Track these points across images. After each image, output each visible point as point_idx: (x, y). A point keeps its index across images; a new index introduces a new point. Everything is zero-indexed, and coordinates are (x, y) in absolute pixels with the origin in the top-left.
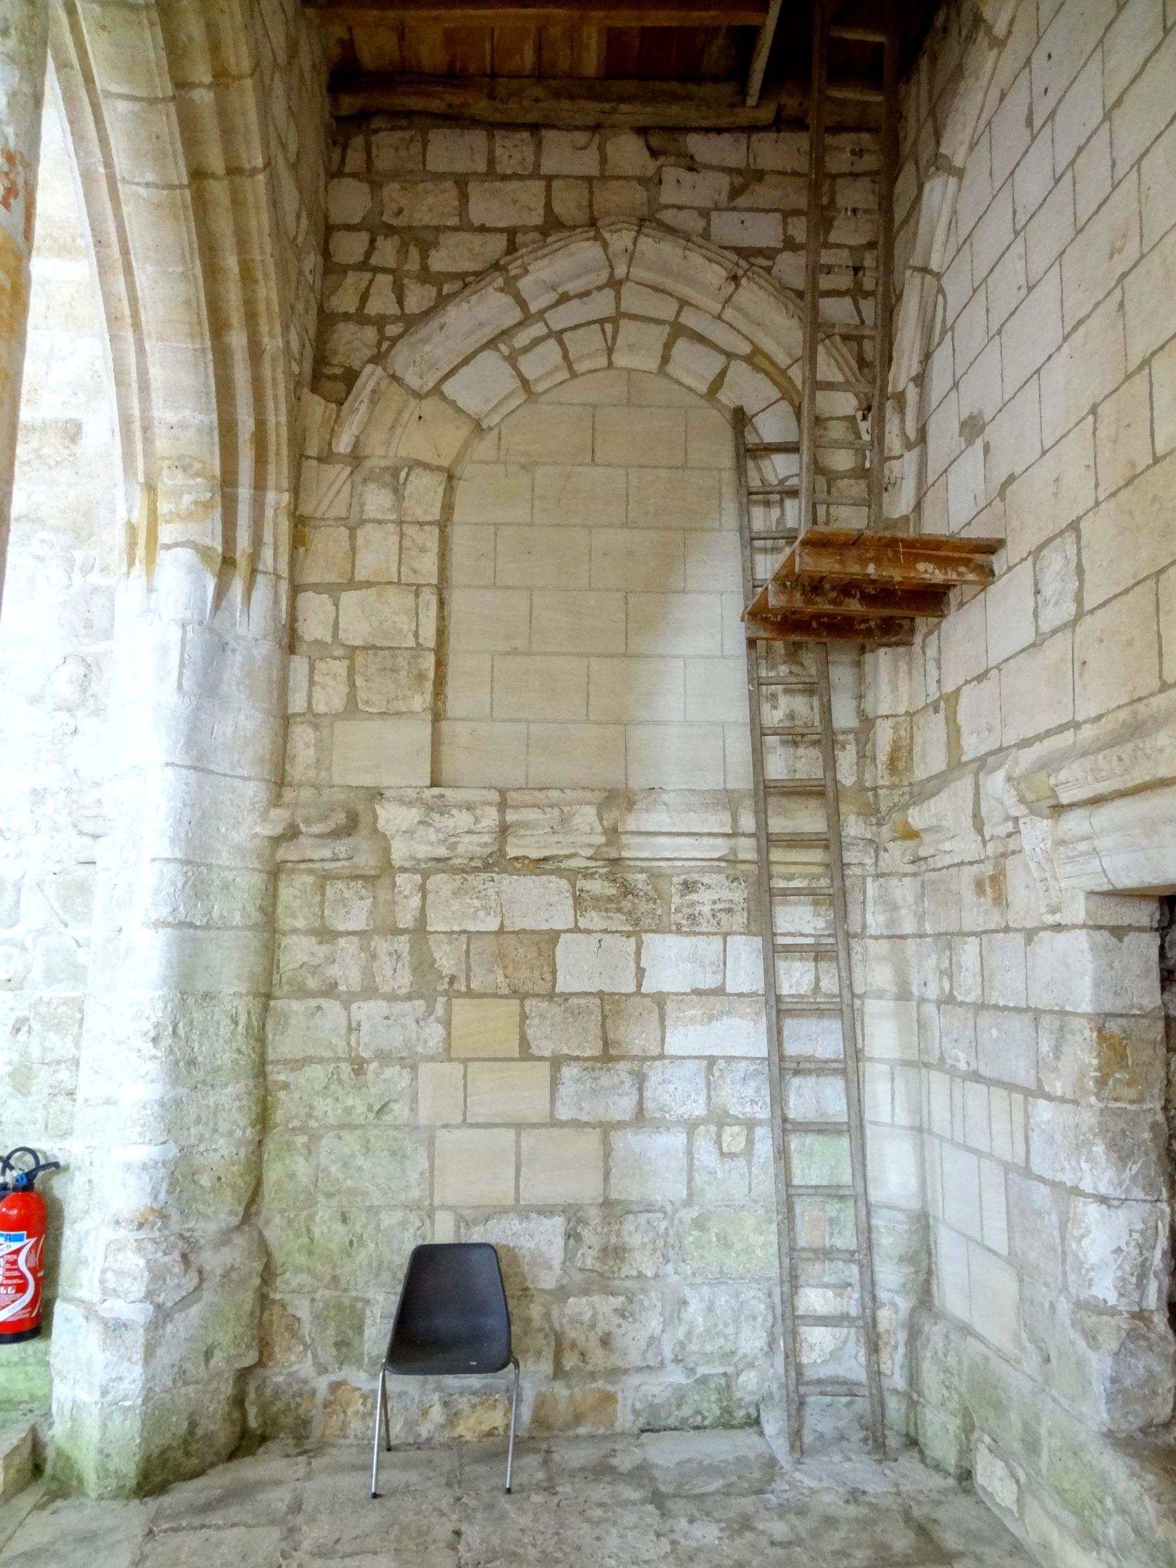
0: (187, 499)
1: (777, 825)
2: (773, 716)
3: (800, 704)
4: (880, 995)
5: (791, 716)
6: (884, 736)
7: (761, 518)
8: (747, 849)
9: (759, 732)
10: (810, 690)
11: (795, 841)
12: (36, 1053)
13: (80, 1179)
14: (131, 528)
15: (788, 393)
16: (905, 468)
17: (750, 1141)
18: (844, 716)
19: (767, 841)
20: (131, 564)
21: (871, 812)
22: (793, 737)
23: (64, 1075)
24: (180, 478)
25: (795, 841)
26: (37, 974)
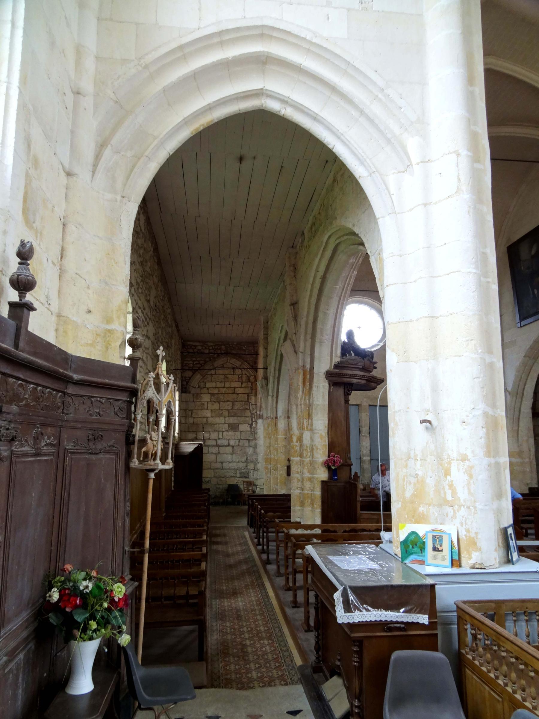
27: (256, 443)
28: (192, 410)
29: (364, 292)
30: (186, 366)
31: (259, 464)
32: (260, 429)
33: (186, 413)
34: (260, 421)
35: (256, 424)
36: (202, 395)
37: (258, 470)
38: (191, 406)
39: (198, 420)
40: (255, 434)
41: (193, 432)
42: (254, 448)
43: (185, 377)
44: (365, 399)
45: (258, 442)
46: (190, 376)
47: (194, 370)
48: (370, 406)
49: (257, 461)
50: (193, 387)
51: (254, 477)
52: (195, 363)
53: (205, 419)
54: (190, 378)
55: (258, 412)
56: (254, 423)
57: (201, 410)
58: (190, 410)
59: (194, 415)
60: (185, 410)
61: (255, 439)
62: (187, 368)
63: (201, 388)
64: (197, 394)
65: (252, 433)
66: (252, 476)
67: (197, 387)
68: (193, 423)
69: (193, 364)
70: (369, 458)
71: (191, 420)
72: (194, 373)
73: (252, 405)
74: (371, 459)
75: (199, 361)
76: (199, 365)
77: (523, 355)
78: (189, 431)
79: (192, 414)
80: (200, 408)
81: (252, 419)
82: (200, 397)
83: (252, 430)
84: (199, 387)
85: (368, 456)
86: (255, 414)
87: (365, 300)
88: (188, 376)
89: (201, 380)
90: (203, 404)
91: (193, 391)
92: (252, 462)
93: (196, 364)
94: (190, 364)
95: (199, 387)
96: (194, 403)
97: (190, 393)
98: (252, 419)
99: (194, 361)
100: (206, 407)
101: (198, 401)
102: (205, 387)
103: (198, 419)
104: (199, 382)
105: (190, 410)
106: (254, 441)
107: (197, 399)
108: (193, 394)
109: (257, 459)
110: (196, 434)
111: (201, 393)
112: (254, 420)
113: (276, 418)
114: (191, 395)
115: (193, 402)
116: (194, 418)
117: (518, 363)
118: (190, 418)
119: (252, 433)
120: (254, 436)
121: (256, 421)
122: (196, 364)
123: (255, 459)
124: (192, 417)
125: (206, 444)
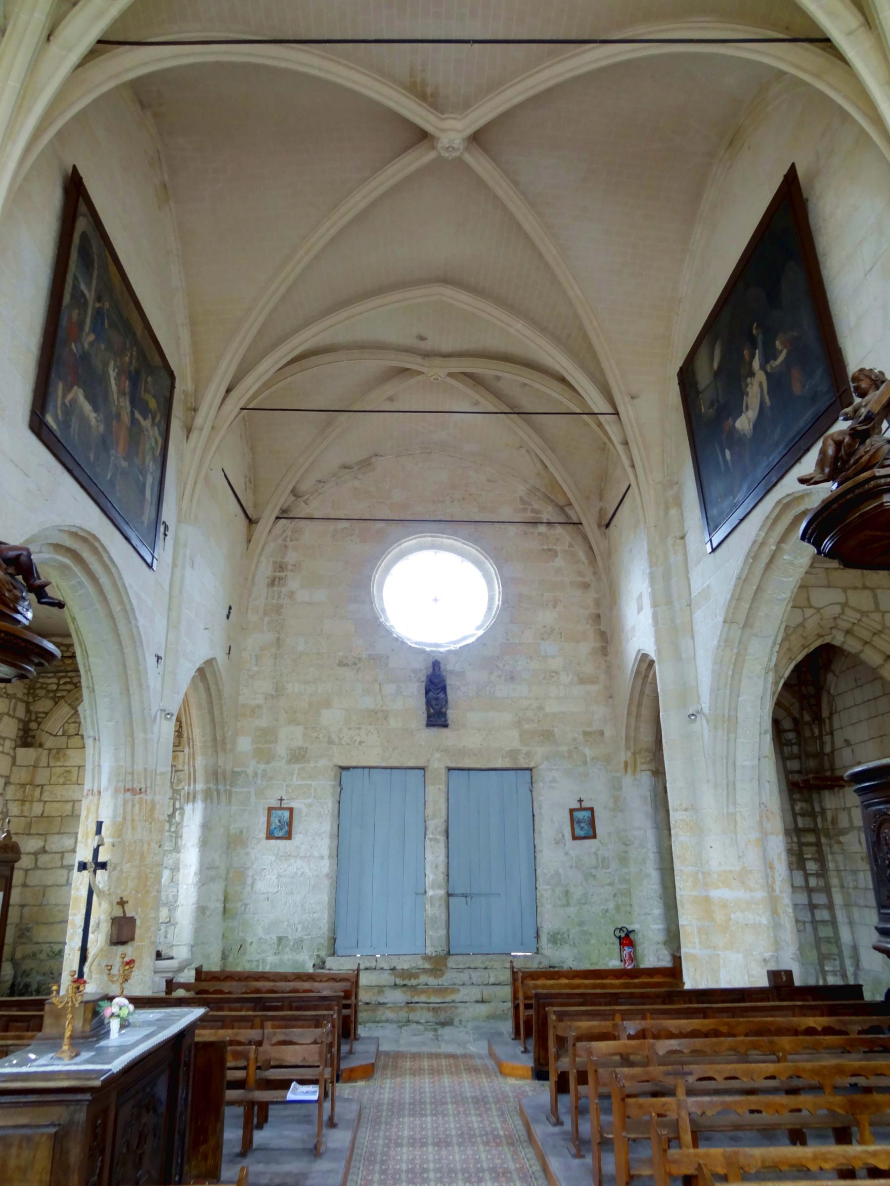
0: (648, 759)
1: (803, 840)
2: (798, 808)
3: (804, 805)
4: (836, 887)
5: (802, 808)
6: (829, 815)
7: (787, 750)
8: (795, 847)
9: (795, 815)
10: (806, 801)
11: (809, 844)
12: (620, 902)
13: (640, 935)
14: (626, 763)
15: (790, 714)
16: (827, 739)
17: (805, 927)
18: (817, 809)
19: (801, 845)
20: (626, 771)
21: (828, 836)
22: (803, 815)
23: (628, 908)
24: (647, 753)
25: (809, 844)
26: (617, 880)
27: (178, 859)
28: (42, 786)
29: (442, 525)
30: (41, 688)
31: (179, 909)
32: (187, 826)
33: (24, 792)
34: (188, 808)
35: (182, 815)
36: (69, 752)
37: (177, 923)
38: (42, 776)
39: (52, 809)
40: (177, 837)
41: (38, 834)
42: (172, 870)
43: (37, 713)
44: (437, 755)
45: (182, 856)
46: (46, 710)
47: (59, 697)
48: (450, 769)
49: (176, 901)
50: (51, 734)
51: (167, 941)
52: (62, 682)
53: (69, 806)
54: (46, 713)
55: (186, 788)
56: (177, 813)
57: (64, 784)
58: (38, 786)
59: (45, 797)
60: (23, 785)
61: (177, 849)
62: (42, 693)
63: (69, 736)
64: (59, 750)
65: (171, 836)
66: (162, 939)
67: (60, 733)
68: (42, 816)
69: (58, 684)
70: (442, 892)
71: (37, 809)
72: (56, 703)
73: (176, 771)
74: (449, 895)
75: (71, 677)
76: (69, 687)
77: (720, 619)
78: (29, 834)
79: (41, 795)
80: (61, 780)
81: (174, 804)
82: (65, 755)
83: (173, 829)
84: (63, 735)
85: (439, 887)
86: (182, 793)
87: (447, 541)
88: (42, 710)
89: (70, 718)
90: (69, 772)
91: (49, 742)
92: (165, 904)
93: (65, 683)
94: (52, 684)
95: (63, 735)
96: (49, 769)
97: (41, 746)
98: (174, 804)
99: (59, 678)
100: (74, 779)
101: (58, 764)
102: (77, 734)
103: (55, 805)
104: (66, 722)
105: (38, 786)
106: (174, 855)
107: (58, 760)
108: (50, 750)
109: (176, 897)
110: (46, 841)
111: (67, 748)
112: (178, 805)
113: (99, 792)
114: (46, 752)
115: (48, 766)
116: (45, 802)
117: (715, 642)
118: (35, 804)
119: (171, 836)
120: (176, 843)
121: (181, 808)
122: (65, 683)
123: (174, 896)
124: (40, 801)
125: (65, 863)
